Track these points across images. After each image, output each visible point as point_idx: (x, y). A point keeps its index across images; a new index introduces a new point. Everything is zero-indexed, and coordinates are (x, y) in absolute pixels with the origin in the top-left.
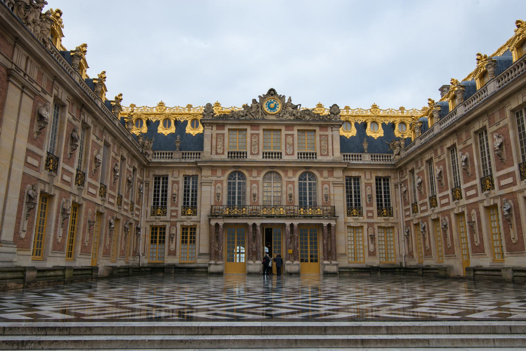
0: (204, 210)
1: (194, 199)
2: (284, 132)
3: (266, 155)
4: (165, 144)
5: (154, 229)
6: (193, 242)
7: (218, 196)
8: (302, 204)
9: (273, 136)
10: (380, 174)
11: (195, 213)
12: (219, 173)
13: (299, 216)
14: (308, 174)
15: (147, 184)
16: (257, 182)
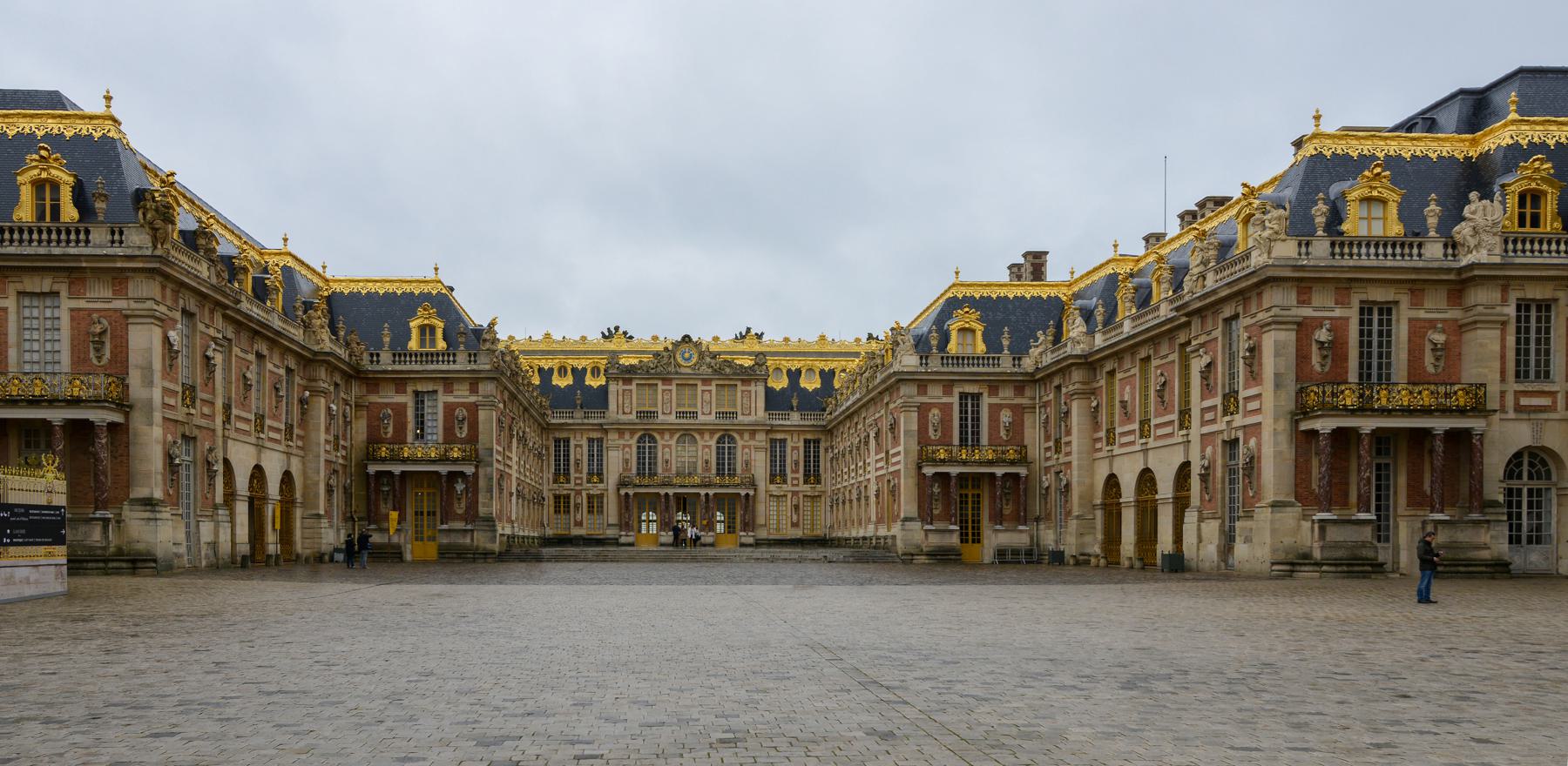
0: (612, 478)
1: (600, 464)
2: (700, 388)
3: (681, 415)
4: (563, 400)
5: (557, 497)
6: (601, 511)
7: (626, 461)
8: (720, 473)
9: (687, 391)
10: (809, 436)
11: (601, 481)
12: (627, 436)
13: (715, 485)
14: (726, 438)
15: (547, 449)
16: (669, 446)
